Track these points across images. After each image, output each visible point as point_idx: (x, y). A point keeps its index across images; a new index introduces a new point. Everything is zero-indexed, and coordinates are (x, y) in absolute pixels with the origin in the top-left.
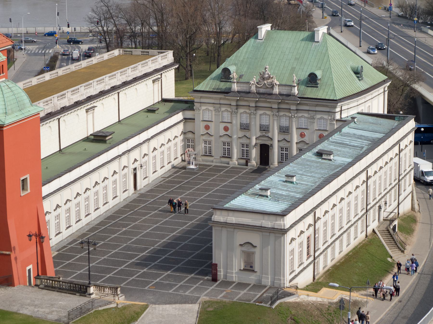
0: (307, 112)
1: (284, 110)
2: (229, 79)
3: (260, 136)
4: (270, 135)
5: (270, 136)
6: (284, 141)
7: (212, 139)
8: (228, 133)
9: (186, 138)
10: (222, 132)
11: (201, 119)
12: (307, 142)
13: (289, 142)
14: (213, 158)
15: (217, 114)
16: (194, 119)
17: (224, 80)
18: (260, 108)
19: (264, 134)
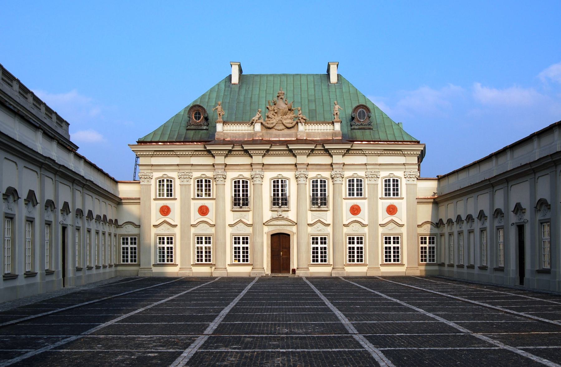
0: (364, 167)
1: (318, 167)
2: (201, 125)
3: (273, 219)
4: (292, 215)
5: (290, 218)
6: (319, 224)
7: (177, 231)
8: (210, 218)
9: (121, 235)
10: (195, 217)
11: (153, 196)
12: (365, 223)
13: (328, 225)
14: (179, 266)
15: (185, 183)
16: (139, 199)
17: (192, 127)
18: (272, 167)
19: (280, 213)
